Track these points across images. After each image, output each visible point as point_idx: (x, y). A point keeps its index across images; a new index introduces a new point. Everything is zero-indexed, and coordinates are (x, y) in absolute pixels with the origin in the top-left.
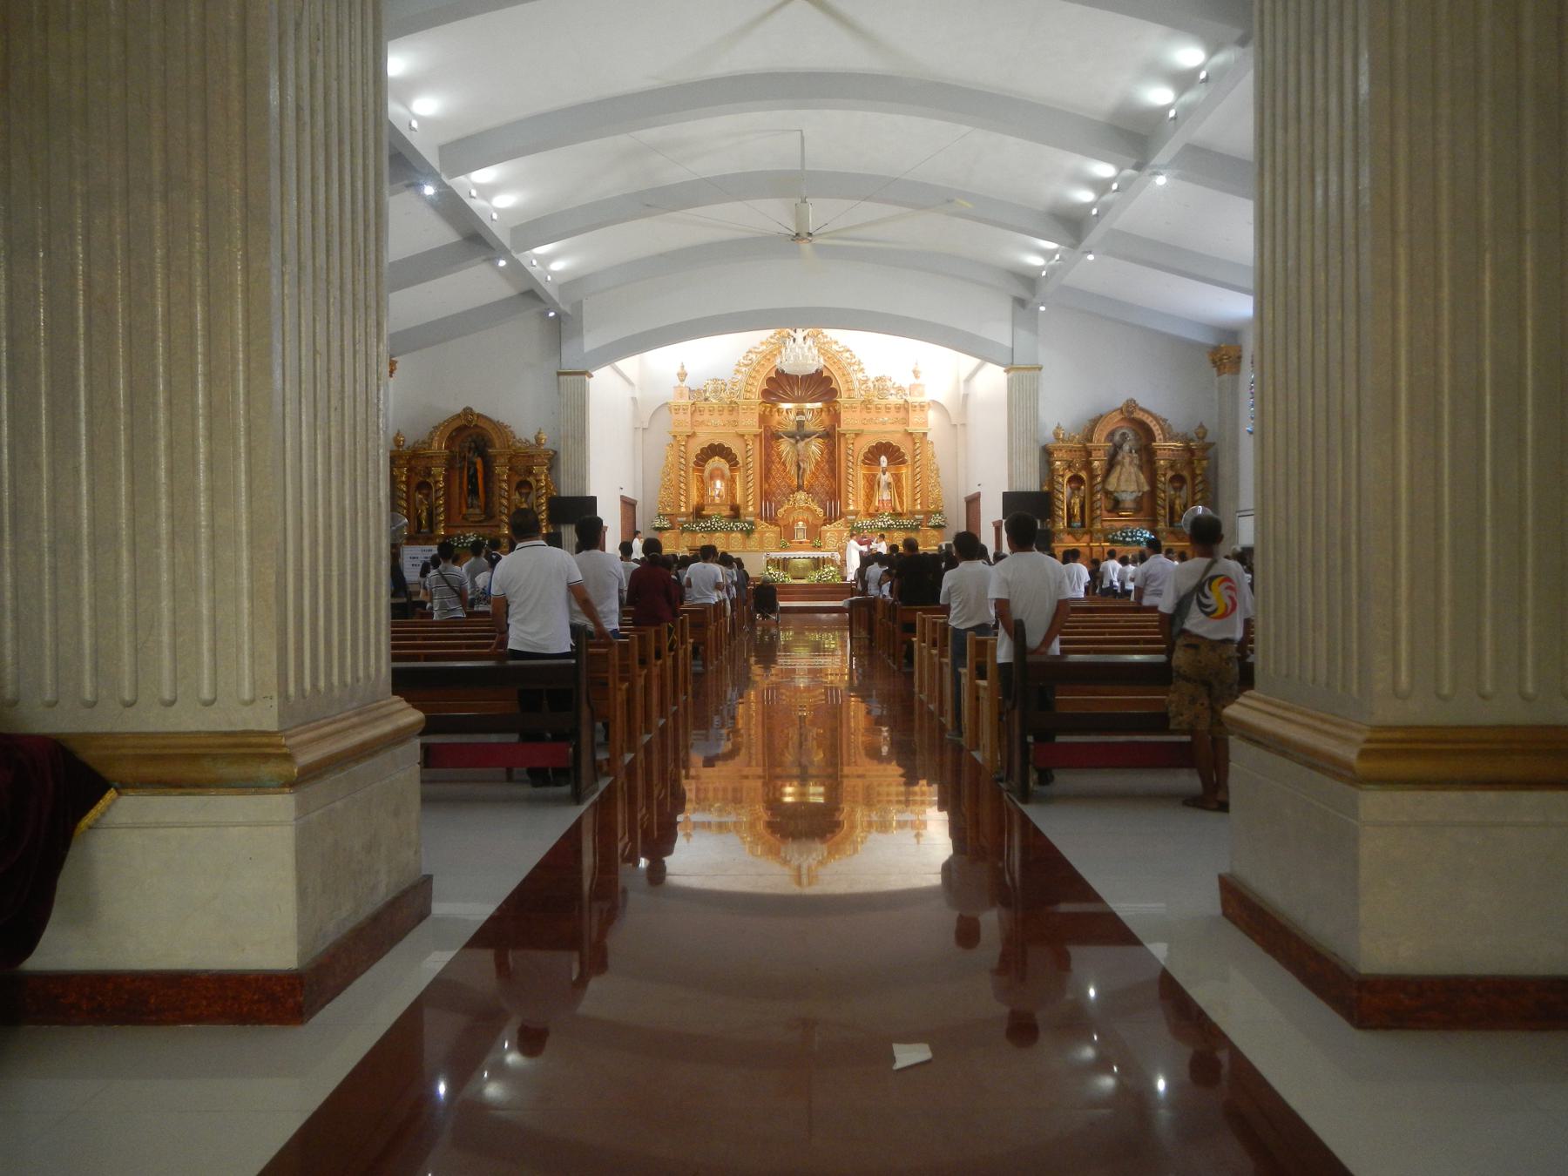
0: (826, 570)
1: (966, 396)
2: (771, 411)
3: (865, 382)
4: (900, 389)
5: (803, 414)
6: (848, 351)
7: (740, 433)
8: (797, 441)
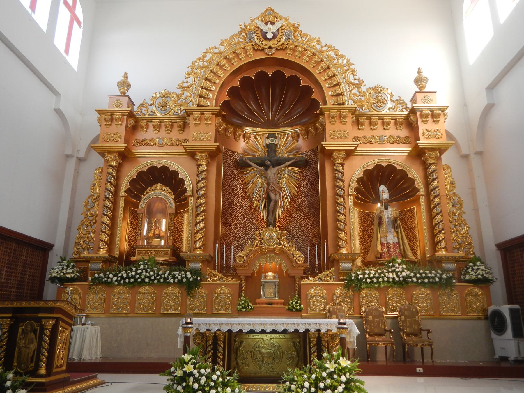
0: (331, 366)
1: (489, 109)
2: (235, 133)
4: (400, 102)
6: (334, 50)
7: (188, 150)
8: (267, 168)
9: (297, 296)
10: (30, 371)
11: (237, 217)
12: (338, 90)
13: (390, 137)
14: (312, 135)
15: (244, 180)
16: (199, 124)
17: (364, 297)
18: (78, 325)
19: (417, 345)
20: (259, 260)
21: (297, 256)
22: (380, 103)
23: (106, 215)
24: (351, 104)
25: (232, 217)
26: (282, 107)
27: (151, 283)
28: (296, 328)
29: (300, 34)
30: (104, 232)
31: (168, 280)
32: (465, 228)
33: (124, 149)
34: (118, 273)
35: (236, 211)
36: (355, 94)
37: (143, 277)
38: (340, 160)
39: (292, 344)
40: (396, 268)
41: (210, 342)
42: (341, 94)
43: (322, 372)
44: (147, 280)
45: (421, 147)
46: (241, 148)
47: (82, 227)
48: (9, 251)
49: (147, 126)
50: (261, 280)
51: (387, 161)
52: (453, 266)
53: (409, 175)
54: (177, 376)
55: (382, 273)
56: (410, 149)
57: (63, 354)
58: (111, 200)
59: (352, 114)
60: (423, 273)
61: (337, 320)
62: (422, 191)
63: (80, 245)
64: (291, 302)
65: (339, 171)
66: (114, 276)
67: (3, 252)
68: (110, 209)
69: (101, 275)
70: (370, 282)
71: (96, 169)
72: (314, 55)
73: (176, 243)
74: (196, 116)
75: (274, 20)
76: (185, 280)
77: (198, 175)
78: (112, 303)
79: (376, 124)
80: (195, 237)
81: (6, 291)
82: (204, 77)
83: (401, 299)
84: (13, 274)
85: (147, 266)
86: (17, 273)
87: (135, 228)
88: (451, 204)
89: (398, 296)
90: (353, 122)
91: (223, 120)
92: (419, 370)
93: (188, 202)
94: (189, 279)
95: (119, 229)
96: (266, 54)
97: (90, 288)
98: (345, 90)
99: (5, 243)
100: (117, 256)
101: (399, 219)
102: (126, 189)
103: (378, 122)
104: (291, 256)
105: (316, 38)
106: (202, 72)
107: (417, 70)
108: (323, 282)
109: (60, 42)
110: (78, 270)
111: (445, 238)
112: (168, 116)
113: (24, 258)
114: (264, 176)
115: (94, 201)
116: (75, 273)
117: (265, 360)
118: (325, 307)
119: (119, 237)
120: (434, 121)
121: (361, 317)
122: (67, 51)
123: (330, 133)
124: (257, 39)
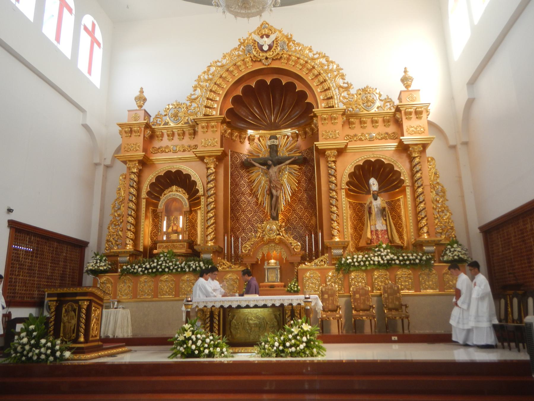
0: (295, 330)
1: (470, 103)
2: (240, 137)
3: (347, 89)
4: (388, 100)
5: (276, 138)
6: (324, 57)
7: (198, 155)
8: (269, 167)
9: (295, 279)
10: (73, 339)
11: (245, 212)
12: (329, 94)
13: (379, 134)
14: (309, 135)
15: (250, 179)
16: (207, 131)
17: (353, 279)
18: (112, 308)
19: (395, 318)
20: (262, 250)
21: (295, 245)
22: (369, 103)
23: (131, 215)
24: (342, 106)
25: (240, 212)
26: (283, 109)
27: (170, 272)
28: (273, 302)
29: (294, 44)
30: (130, 230)
31: (184, 270)
32: (447, 215)
33: (143, 157)
34: (142, 264)
35: (243, 207)
36: (344, 97)
37: (163, 267)
38: (333, 158)
39: (273, 317)
40: (382, 252)
41: (208, 316)
42: (331, 98)
43: (289, 334)
44: (167, 270)
45: (405, 143)
46: (247, 150)
47: (112, 226)
48: (52, 249)
49: (162, 135)
50: (264, 267)
51: (375, 156)
52: (432, 249)
53: (396, 168)
54: (179, 340)
55: (369, 257)
56: (396, 144)
57: (97, 328)
58: (135, 202)
59: (344, 114)
60: (405, 256)
61: (303, 296)
62: (408, 182)
63: (110, 241)
64: (290, 284)
65: (331, 168)
66: (139, 267)
67: (47, 251)
68: (133, 210)
69: (129, 266)
70: (358, 266)
71: (121, 176)
72: (306, 62)
73: (193, 237)
74: (203, 124)
75: (269, 33)
76: (198, 268)
77: (208, 176)
78: (138, 289)
79: (365, 123)
80: (207, 231)
81: (51, 282)
82: (209, 89)
83: (386, 280)
84: (56, 268)
85: (166, 258)
86: (59, 267)
87: (157, 225)
88: (434, 192)
89: (383, 277)
90: (344, 122)
91: (228, 126)
92: (394, 338)
93: (200, 202)
94: (202, 268)
95: (142, 227)
96: (263, 64)
97: (120, 278)
98: (334, 94)
99: (48, 243)
100: (142, 250)
101: (387, 209)
102: (147, 191)
103: (367, 121)
104: (289, 245)
105: (308, 47)
106: (208, 84)
107: (404, 70)
108: (318, 267)
109: (82, 65)
110: (110, 263)
111: (427, 224)
112: (180, 125)
113: (65, 254)
114: (266, 174)
115: (120, 203)
116: (107, 265)
117: (253, 329)
118: (319, 288)
119: (142, 234)
120: (417, 118)
121: (351, 296)
122: (90, 72)
123: (323, 133)
124: (255, 51)
